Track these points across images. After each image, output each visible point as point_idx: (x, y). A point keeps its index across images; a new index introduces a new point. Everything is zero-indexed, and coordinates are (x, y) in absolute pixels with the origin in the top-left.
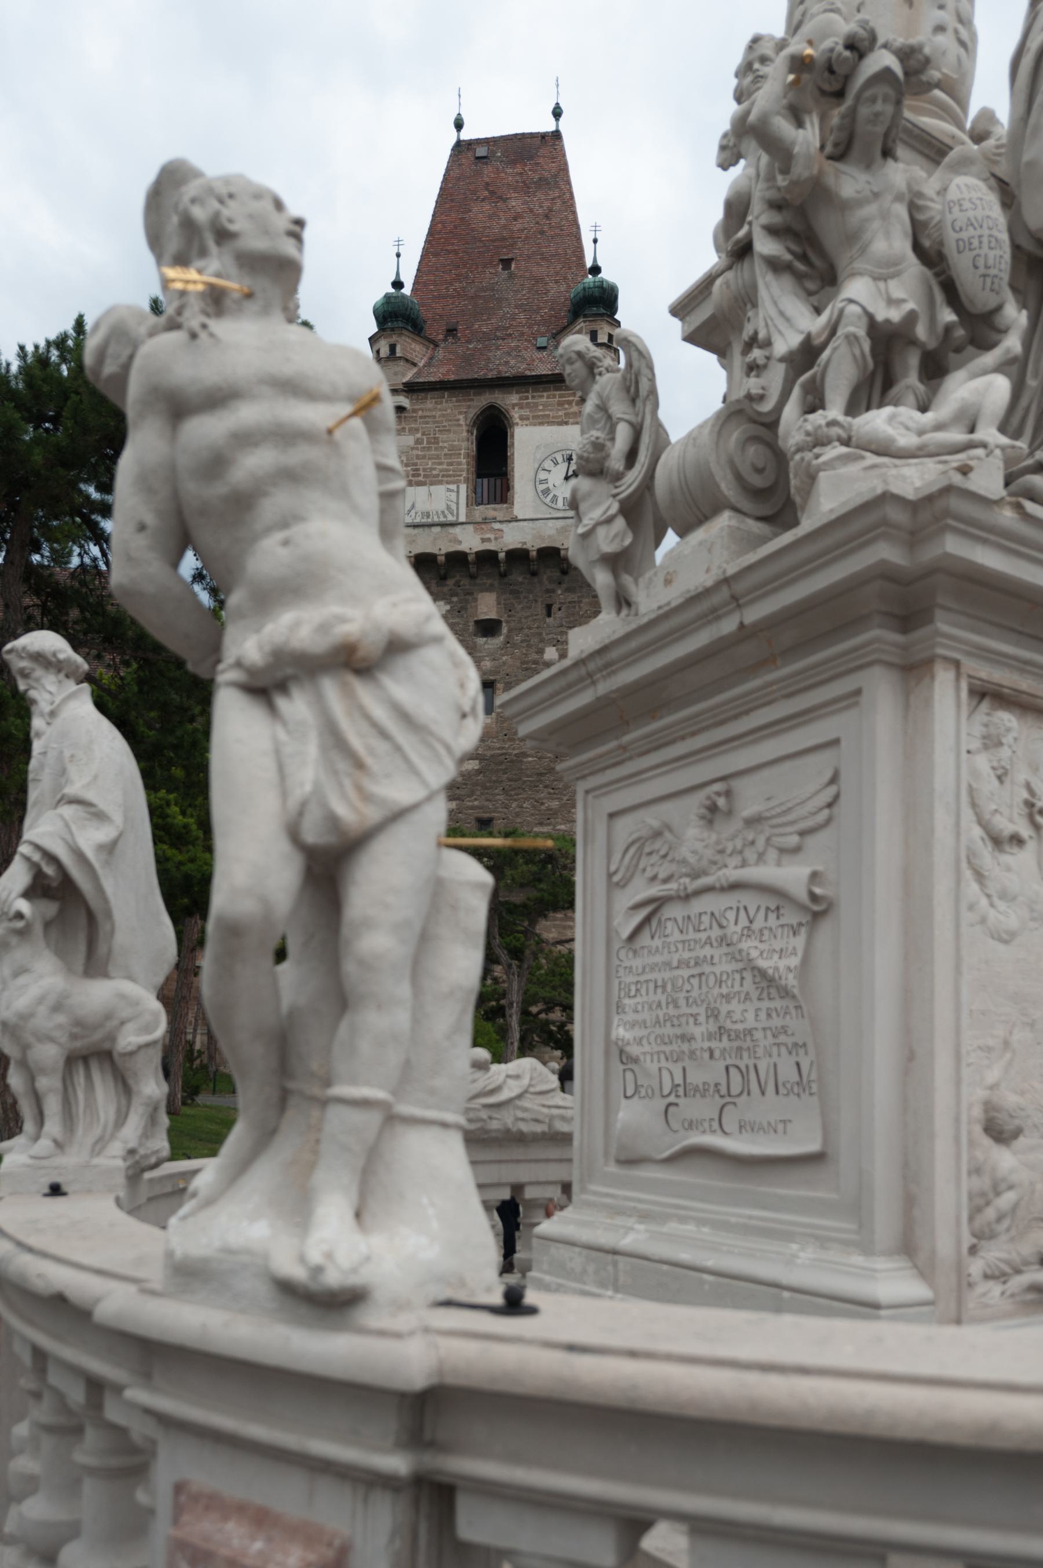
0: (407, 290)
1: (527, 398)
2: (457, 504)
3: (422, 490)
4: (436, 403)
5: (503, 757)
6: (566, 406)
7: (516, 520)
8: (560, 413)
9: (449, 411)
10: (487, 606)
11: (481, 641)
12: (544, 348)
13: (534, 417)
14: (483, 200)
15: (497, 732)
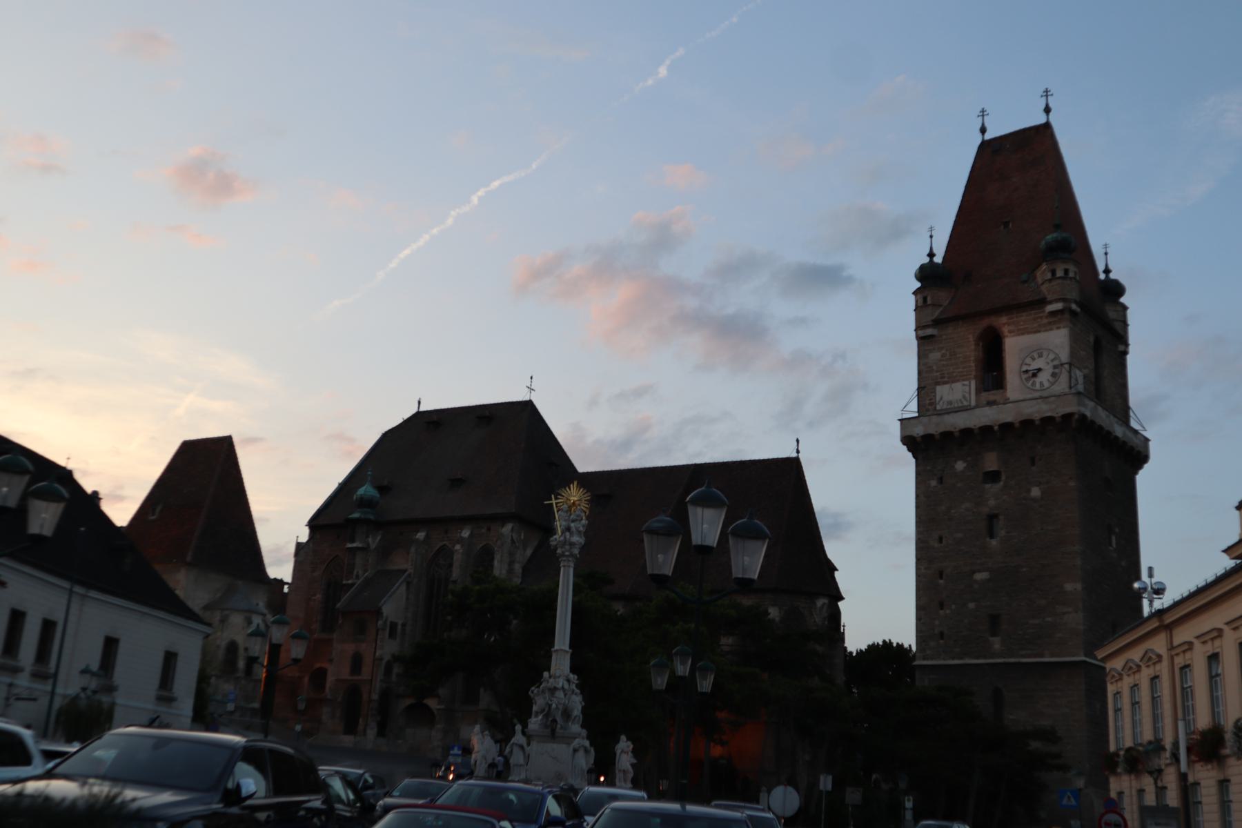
0: (938, 259)
3: (947, 387)
10: (991, 462)
11: (988, 486)
12: (1025, 282)
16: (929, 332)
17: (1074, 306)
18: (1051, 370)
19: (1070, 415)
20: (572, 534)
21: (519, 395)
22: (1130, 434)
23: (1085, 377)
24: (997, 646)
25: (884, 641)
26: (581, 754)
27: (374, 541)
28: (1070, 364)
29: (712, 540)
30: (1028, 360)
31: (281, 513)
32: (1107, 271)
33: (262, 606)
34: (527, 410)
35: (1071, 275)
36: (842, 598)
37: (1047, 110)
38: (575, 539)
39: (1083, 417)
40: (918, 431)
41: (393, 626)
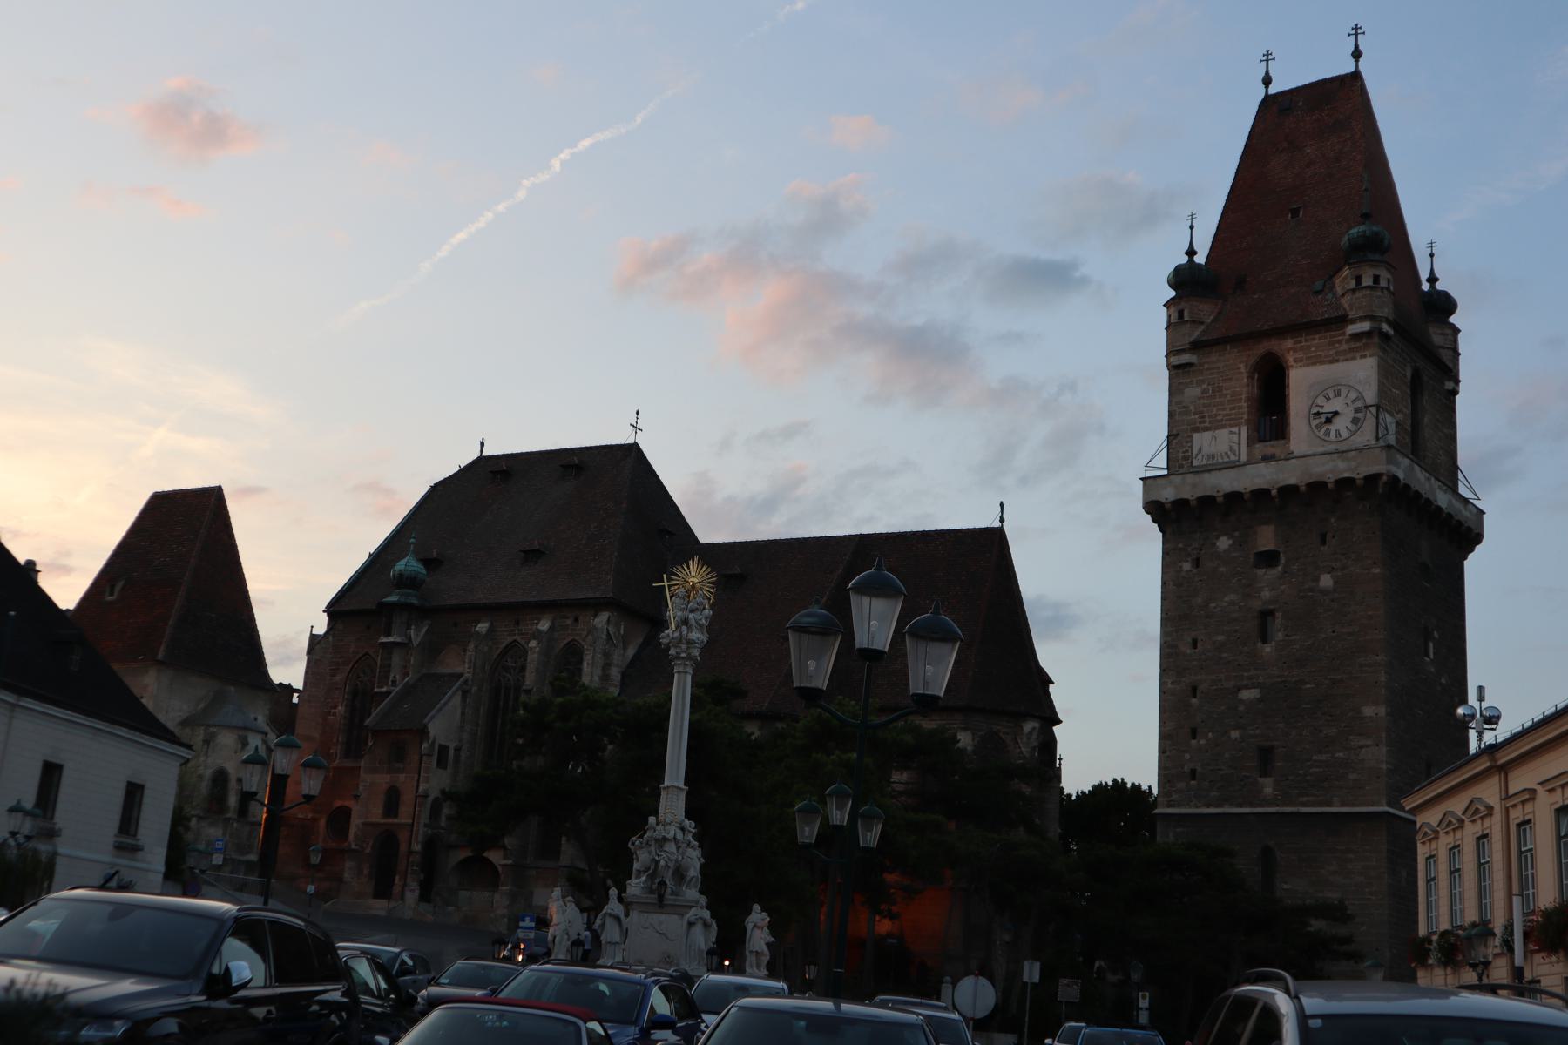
0: (1200, 259)
3: (1208, 434)
7: (1289, 456)
10: (1266, 538)
11: (1261, 572)
12: (1321, 291)
16: (1186, 358)
17: (1385, 327)
18: (1351, 415)
19: (1377, 476)
20: (690, 628)
21: (622, 437)
22: (1457, 504)
23: (1398, 424)
24: (1268, 790)
25: (1115, 781)
26: (698, 928)
27: (417, 635)
28: (1378, 407)
29: (883, 641)
30: (1320, 401)
31: (290, 593)
32: (1433, 279)
33: (262, 721)
34: (631, 455)
35: (1383, 283)
36: (1059, 722)
37: (1357, 54)
38: (695, 635)
39: (1395, 479)
40: (1167, 495)
41: (443, 750)
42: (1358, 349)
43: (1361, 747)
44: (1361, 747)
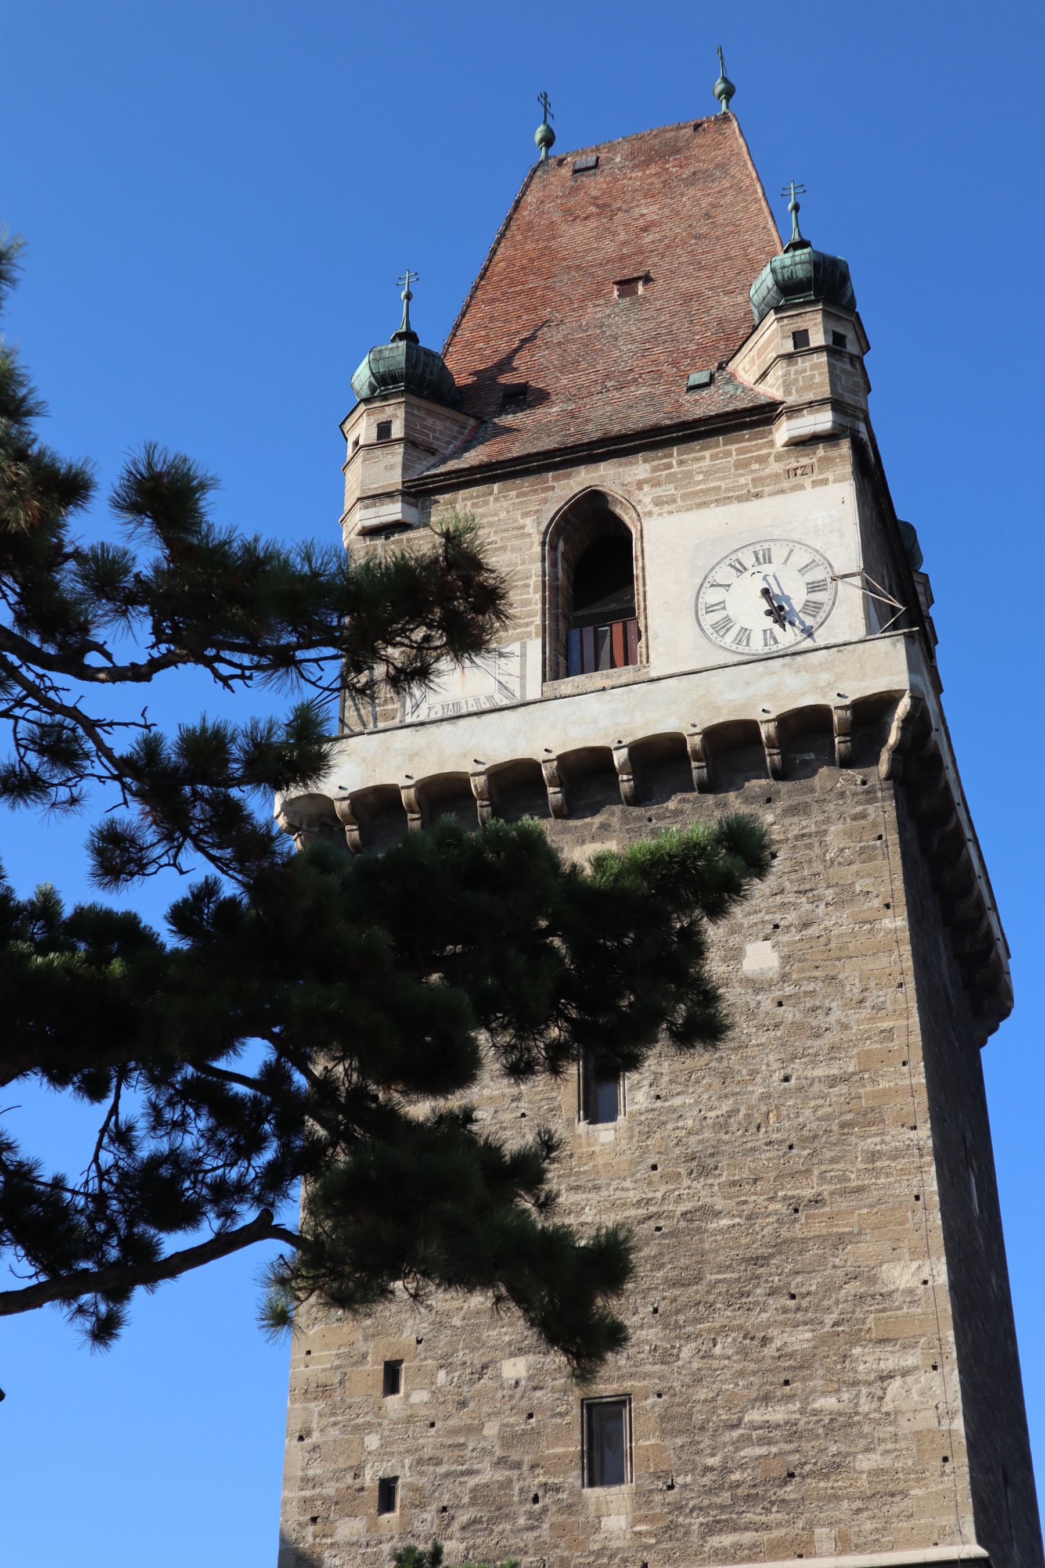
1: (669, 466)
2: (523, 677)
4: (474, 505)
5: (652, 1224)
6: (755, 466)
8: (742, 481)
9: (503, 515)
13: (684, 497)
14: (586, 218)
15: (635, 1163)
19: (886, 701)
42: (806, 470)
43: (886, 1377)
44: (886, 1377)
